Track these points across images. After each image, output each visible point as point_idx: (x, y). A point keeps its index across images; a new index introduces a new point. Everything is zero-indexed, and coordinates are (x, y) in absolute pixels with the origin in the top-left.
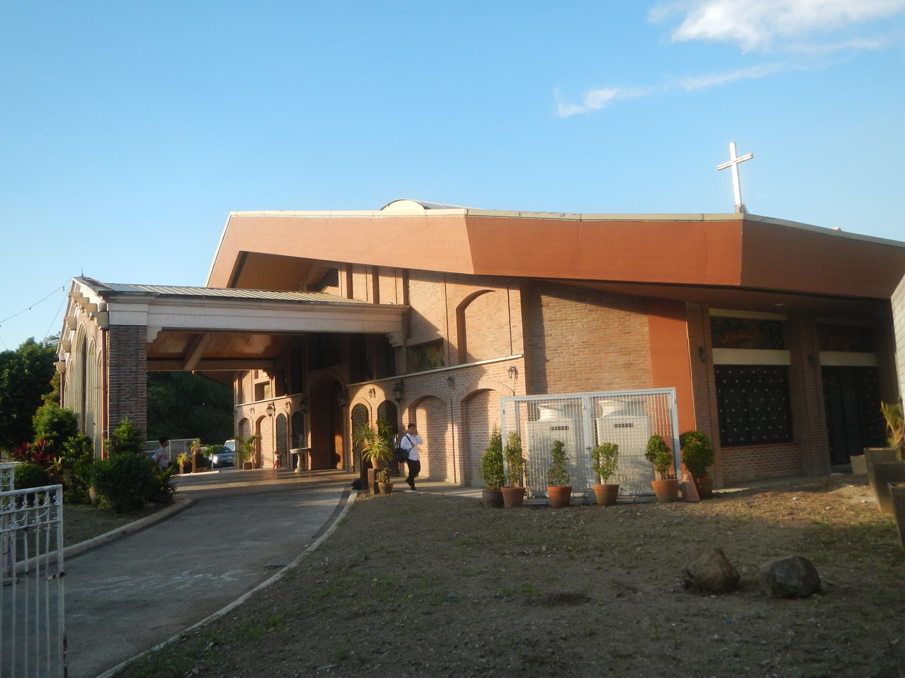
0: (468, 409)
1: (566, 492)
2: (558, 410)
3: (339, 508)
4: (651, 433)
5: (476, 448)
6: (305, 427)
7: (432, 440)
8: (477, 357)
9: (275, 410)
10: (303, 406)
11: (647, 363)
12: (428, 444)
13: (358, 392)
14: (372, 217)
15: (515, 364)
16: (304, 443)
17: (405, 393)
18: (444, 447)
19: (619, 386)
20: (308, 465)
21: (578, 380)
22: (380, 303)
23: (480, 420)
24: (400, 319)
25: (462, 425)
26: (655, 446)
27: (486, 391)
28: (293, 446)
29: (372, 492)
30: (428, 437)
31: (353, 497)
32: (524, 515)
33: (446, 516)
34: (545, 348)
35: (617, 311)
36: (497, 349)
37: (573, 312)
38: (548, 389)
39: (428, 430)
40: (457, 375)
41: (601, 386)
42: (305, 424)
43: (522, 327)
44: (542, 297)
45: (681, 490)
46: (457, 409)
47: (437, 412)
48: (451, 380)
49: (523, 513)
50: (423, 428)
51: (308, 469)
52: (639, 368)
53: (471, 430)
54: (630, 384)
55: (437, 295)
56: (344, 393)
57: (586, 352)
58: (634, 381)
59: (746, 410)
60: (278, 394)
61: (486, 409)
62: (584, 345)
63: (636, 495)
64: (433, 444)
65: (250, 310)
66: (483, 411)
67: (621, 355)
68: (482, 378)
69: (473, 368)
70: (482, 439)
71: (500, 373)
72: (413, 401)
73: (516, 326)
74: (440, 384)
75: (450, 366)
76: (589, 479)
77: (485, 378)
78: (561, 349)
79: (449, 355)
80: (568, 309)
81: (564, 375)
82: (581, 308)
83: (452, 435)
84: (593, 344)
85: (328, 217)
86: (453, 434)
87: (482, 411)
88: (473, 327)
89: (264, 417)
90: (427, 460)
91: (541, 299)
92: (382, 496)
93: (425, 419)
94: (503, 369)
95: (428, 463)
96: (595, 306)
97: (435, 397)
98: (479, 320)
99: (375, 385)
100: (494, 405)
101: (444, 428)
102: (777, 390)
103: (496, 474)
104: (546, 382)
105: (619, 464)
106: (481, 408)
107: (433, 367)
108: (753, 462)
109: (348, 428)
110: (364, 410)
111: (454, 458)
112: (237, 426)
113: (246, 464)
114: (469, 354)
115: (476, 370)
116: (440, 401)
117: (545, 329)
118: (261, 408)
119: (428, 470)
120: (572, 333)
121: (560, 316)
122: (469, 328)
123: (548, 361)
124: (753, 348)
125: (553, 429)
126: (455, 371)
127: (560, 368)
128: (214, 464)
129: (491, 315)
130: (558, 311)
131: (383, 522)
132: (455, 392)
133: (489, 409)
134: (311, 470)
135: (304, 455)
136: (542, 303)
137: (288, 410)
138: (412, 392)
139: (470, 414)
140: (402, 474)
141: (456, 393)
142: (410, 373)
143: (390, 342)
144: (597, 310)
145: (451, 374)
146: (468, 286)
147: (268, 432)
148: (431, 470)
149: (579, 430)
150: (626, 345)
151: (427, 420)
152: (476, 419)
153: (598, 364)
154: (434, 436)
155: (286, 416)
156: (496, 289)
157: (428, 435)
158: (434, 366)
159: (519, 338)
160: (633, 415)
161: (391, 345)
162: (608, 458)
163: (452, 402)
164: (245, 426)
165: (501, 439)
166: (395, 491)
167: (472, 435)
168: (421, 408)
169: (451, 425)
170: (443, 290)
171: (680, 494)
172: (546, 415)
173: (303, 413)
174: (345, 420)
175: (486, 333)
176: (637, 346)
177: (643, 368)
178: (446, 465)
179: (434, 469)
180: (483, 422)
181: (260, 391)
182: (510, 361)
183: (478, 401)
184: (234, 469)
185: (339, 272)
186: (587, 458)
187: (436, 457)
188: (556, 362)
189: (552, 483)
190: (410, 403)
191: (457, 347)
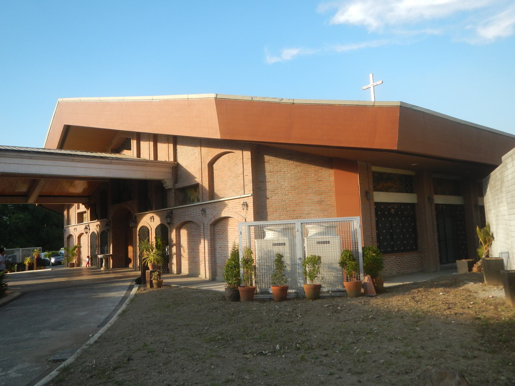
0: (214, 230)
1: (284, 290)
2: (279, 232)
3: (124, 298)
4: (343, 248)
5: (219, 256)
6: (109, 240)
7: (190, 250)
8: (221, 196)
9: (89, 229)
11: (332, 200)
12: (188, 253)
13: (143, 218)
14: (152, 100)
15: (246, 201)
16: (108, 251)
17: (174, 219)
18: (199, 254)
19: (314, 215)
20: (110, 265)
21: (287, 211)
22: (158, 160)
23: (222, 237)
25: (211, 241)
26: (347, 257)
27: (227, 218)
28: (101, 252)
29: (148, 286)
30: (188, 248)
31: (135, 290)
32: (256, 309)
33: (199, 311)
34: (266, 190)
35: (313, 166)
36: (234, 190)
37: (285, 166)
38: (268, 217)
39: (188, 243)
40: (207, 207)
41: (302, 215)
42: (108, 239)
43: (251, 176)
44: (265, 156)
45: (363, 288)
46: (207, 230)
47: (194, 232)
48: (204, 211)
49: (254, 306)
50: (185, 242)
51: (110, 268)
52: (327, 204)
53: (216, 244)
54: (321, 214)
55: (195, 155)
56: (134, 219)
57: (293, 193)
58: (324, 212)
59: (391, 231)
60: (92, 219)
61: (227, 230)
62: (292, 188)
63: (333, 292)
64: (191, 253)
65: (66, 162)
66: (225, 231)
67: (316, 195)
68: (225, 210)
69: (219, 203)
70: (224, 250)
71: (236, 207)
72: (178, 224)
73: (247, 175)
75: (203, 202)
76: (300, 280)
77: (226, 209)
78: (277, 191)
79: (203, 194)
80: (282, 165)
81: (278, 208)
82: (290, 164)
83: (203, 247)
84: (297, 188)
85: (122, 101)
86: (204, 246)
87: (224, 231)
88: (219, 176)
89: (82, 234)
90: (187, 263)
91: (264, 157)
92: (155, 290)
93: (187, 236)
95: (188, 265)
96: (299, 163)
97: (193, 222)
98: (222, 171)
99: (155, 214)
100: (231, 228)
102: (409, 218)
103: (234, 277)
104: (267, 212)
105: (321, 270)
106: (223, 229)
107: (192, 202)
108: (396, 264)
109: (136, 241)
110: (147, 230)
111: (205, 262)
112: (65, 239)
113: (71, 264)
114: (216, 194)
115: (220, 204)
116: (196, 225)
117: (267, 178)
118: (81, 228)
119: (188, 269)
120: (284, 180)
121: (276, 169)
122: (216, 177)
123: (268, 198)
124: (396, 192)
125: (275, 245)
126: (206, 205)
127: (276, 204)
128: (52, 263)
129: (231, 168)
130: (275, 166)
131: (151, 316)
132: (207, 219)
133: (229, 230)
134: (112, 268)
135: (108, 258)
136: (265, 160)
137: (98, 230)
138: (178, 219)
139: (216, 233)
140: (171, 272)
141: (207, 220)
142: (177, 206)
143: (164, 186)
144: (301, 166)
145: (204, 207)
146: (216, 149)
147: (85, 242)
148: (190, 270)
149: (293, 246)
150: (319, 189)
151: (188, 237)
152: (220, 236)
153: (300, 201)
154: (192, 247)
155: (96, 233)
156: (235, 151)
157: (188, 247)
158: (193, 201)
159: (249, 183)
160: (331, 235)
161: (165, 188)
162: (314, 266)
163: (204, 225)
164: (71, 240)
165: (238, 252)
166: (165, 285)
167: (217, 247)
168: (184, 229)
169: (203, 240)
170: (199, 152)
171: (362, 290)
172: (270, 235)
174: (134, 236)
176: (326, 189)
177: (330, 204)
178: (199, 266)
179: (192, 269)
180: (225, 238)
181: (80, 217)
182: (243, 199)
184: (63, 267)
185: (132, 141)
186: (298, 266)
187: (193, 261)
188: (274, 199)
189: (274, 283)
190: (177, 226)
191: (208, 189)
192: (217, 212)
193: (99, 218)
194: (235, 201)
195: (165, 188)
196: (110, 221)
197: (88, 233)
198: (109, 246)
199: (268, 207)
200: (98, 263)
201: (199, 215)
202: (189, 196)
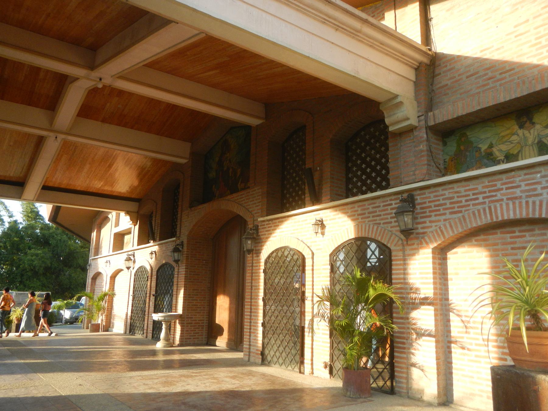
6: (175, 283)
9: (134, 262)
10: (176, 254)
24: (411, 75)
42: (175, 280)
89: (119, 271)
112: (89, 281)
113: (93, 325)
128: (66, 319)
134: (179, 345)
137: (153, 261)
138: (448, 216)
143: (387, 121)
155: (148, 268)
164: (98, 282)
173: (174, 264)
193: (158, 239)
196: (182, 242)
197: (131, 269)
198: (174, 296)
200: (147, 330)
202: (484, 147)
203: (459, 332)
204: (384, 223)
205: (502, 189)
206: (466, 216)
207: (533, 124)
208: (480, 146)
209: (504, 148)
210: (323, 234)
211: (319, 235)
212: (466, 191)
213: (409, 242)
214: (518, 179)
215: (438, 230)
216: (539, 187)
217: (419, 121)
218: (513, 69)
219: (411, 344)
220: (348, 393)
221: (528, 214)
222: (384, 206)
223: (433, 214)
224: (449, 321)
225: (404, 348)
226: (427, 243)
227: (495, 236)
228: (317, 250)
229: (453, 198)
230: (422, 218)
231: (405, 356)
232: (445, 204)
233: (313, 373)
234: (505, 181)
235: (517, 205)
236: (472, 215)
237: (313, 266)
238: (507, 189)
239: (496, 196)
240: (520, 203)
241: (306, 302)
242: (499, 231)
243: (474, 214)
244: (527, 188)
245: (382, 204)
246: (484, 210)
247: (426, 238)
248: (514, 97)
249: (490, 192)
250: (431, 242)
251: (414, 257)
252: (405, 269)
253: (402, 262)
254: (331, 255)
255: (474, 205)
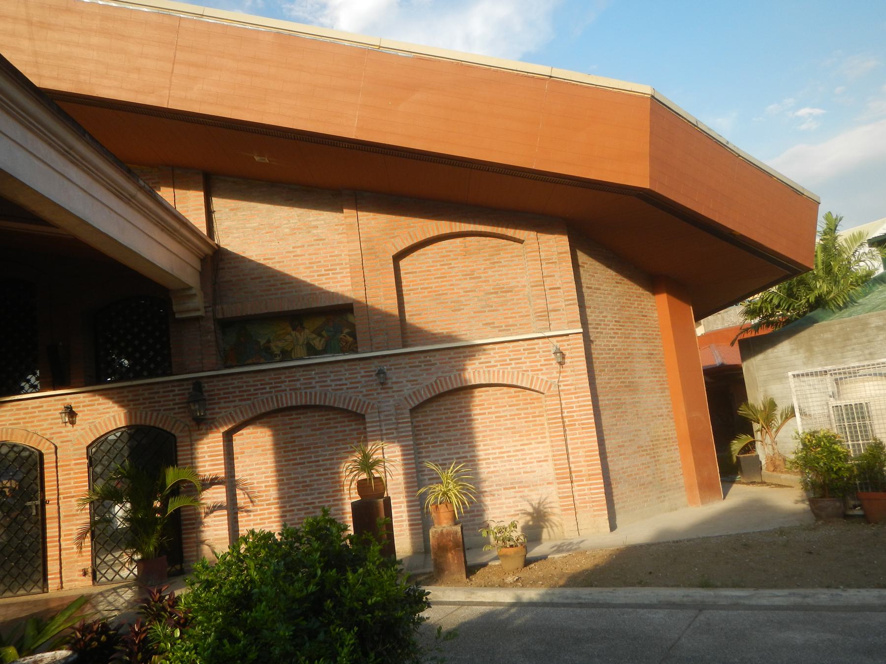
21: (617, 370)
24: (198, 265)
36: (493, 323)
39: (277, 471)
40: (391, 365)
47: (312, 435)
69: (446, 352)
71: (521, 359)
73: (559, 288)
74: (339, 383)
87: (453, 422)
88: (426, 288)
94: (527, 352)
101: (335, 461)
115: (452, 355)
126: (387, 359)
138: (237, 403)
141: (393, 396)
143: (175, 308)
144: (621, 283)
151: (276, 453)
152: (439, 437)
153: (630, 351)
157: (278, 481)
158: (286, 355)
175: (462, 299)
183: (442, 408)
192: (440, 374)
194: (513, 347)
195: (174, 314)
199: (594, 360)
201: (349, 386)
202: (263, 342)
203: (244, 503)
204: (164, 410)
205: (285, 382)
206: (256, 403)
207: (303, 328)
208: (259, 340)
209: (280, 344)
210: (73, 423)
211: (68, 424)
212: (254, 381)
213: (201, 427)
214: (298, 374)
215: (229, 416)
216: (313, 381)
217: (206, 312)
218: (290, 283)
219: (201, 523)
220: (150, 583)
221: (306, 402)
222: (164, 392)
223: (222, 401)
224: (235, 495)
225: (194, 528)
226: (217, 427)
227: (276, 419)
228: (62, 442)
229: (242, 387)
230: (210, 404)
231: (195, 535)
232: (235, 392)
233: (62, 587)
234: (288, 375)
235: (299, 395)
236: (261, 403)
237: (56, 462)
238: (289, 381)
239: (280, 387)
240: (301, 393)
241: (47, 507)
242: (280, 415)
243: (263, 402)
244: (305, 381)
245: (161, 390)
246: (272, 398)
247: (216, 423)
248: (295, 308)
249: (275, 383)
250: (221, 426)
251: (202, 442)
252: (192, 454)
253: (189, 448)
254: (88, 447)
255: (262, 394)
